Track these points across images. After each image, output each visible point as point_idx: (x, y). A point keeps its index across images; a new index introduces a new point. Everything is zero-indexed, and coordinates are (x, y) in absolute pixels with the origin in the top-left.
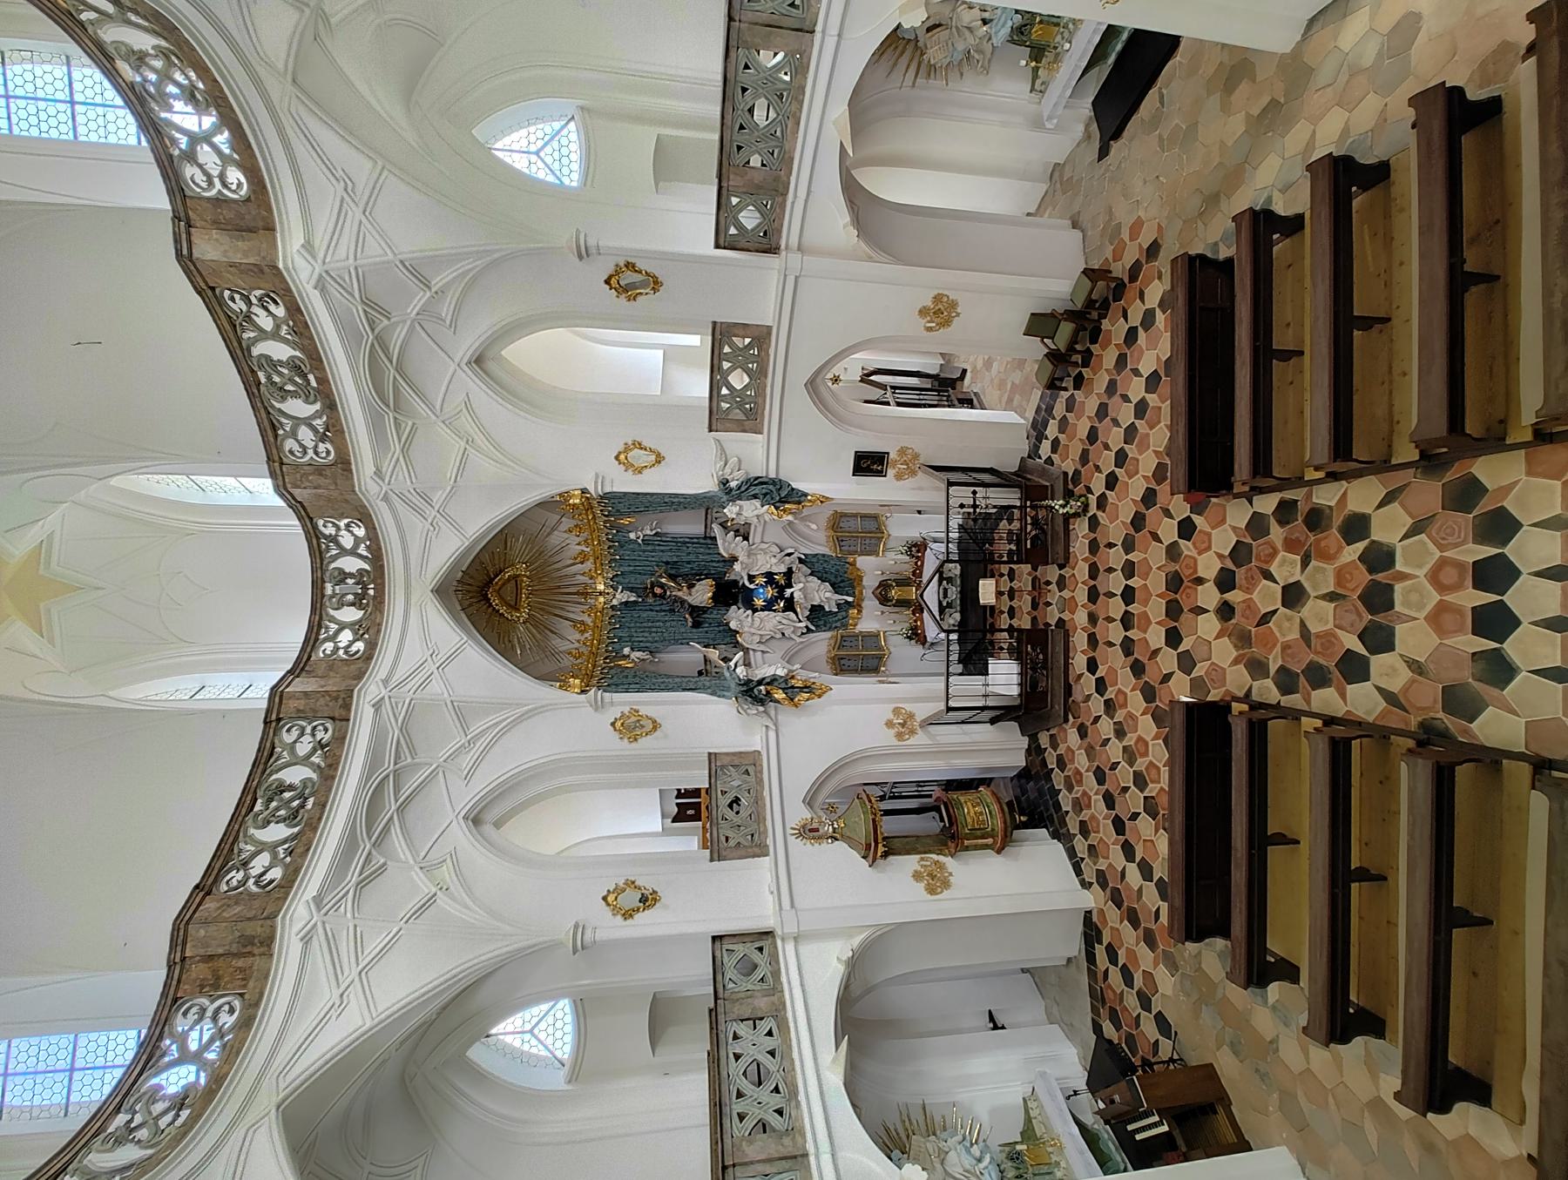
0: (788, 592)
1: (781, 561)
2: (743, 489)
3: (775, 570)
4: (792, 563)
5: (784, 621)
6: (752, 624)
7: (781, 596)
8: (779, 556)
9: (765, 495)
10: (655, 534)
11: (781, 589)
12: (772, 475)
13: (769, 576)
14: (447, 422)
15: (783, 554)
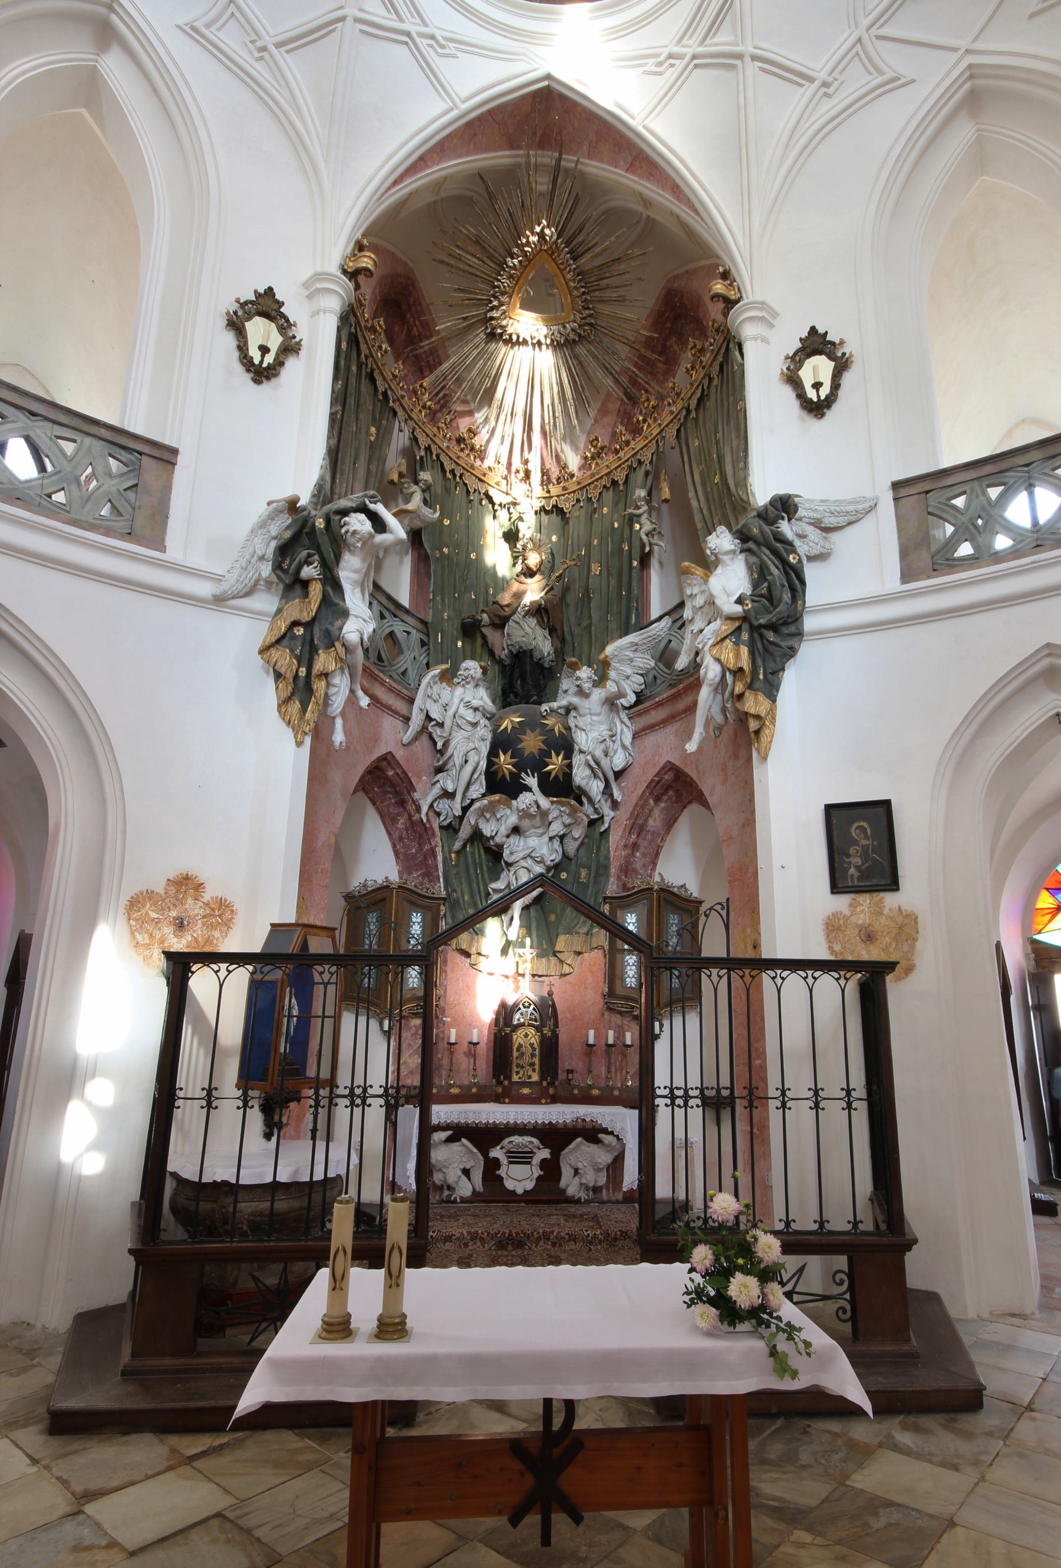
0: (532, 781)
1: (595, 769)
2: (778, 545)
3: (577, 760)
4: (591, 801)
5: (469, 768)
6: (468, 705)
7: (525, 763)
8: (605, 763)
9: (770, 597)
10: (641, 538)
11: (537, 765)
12: (810, 623)
13: (566, 745)
14: (858, 47)
15: (611, 776)
